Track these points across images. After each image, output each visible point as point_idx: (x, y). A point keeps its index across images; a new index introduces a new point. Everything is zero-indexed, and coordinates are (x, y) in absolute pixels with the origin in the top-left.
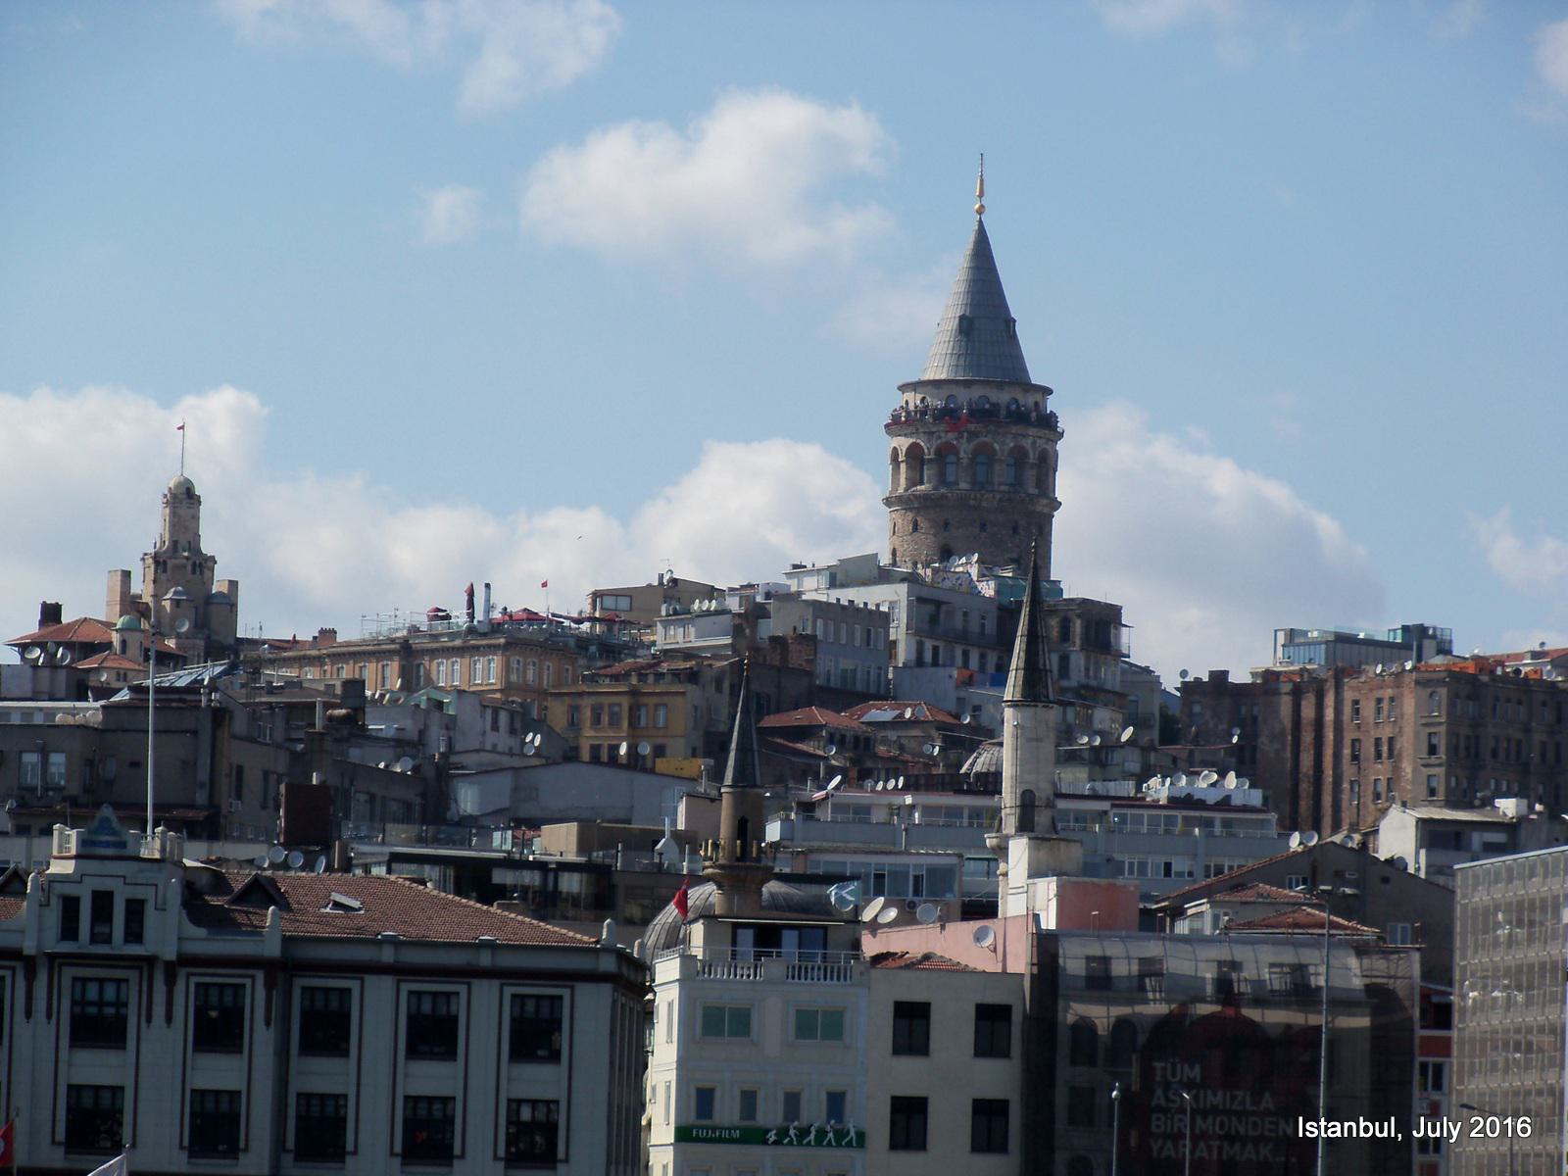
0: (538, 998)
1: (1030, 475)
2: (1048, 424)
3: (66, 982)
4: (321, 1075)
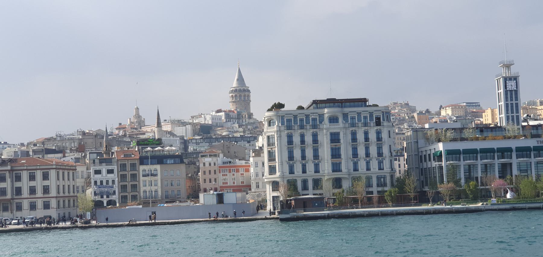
0: (46, 172)
1: (246, 98)
2: (249, 91)
4: (18, 184)
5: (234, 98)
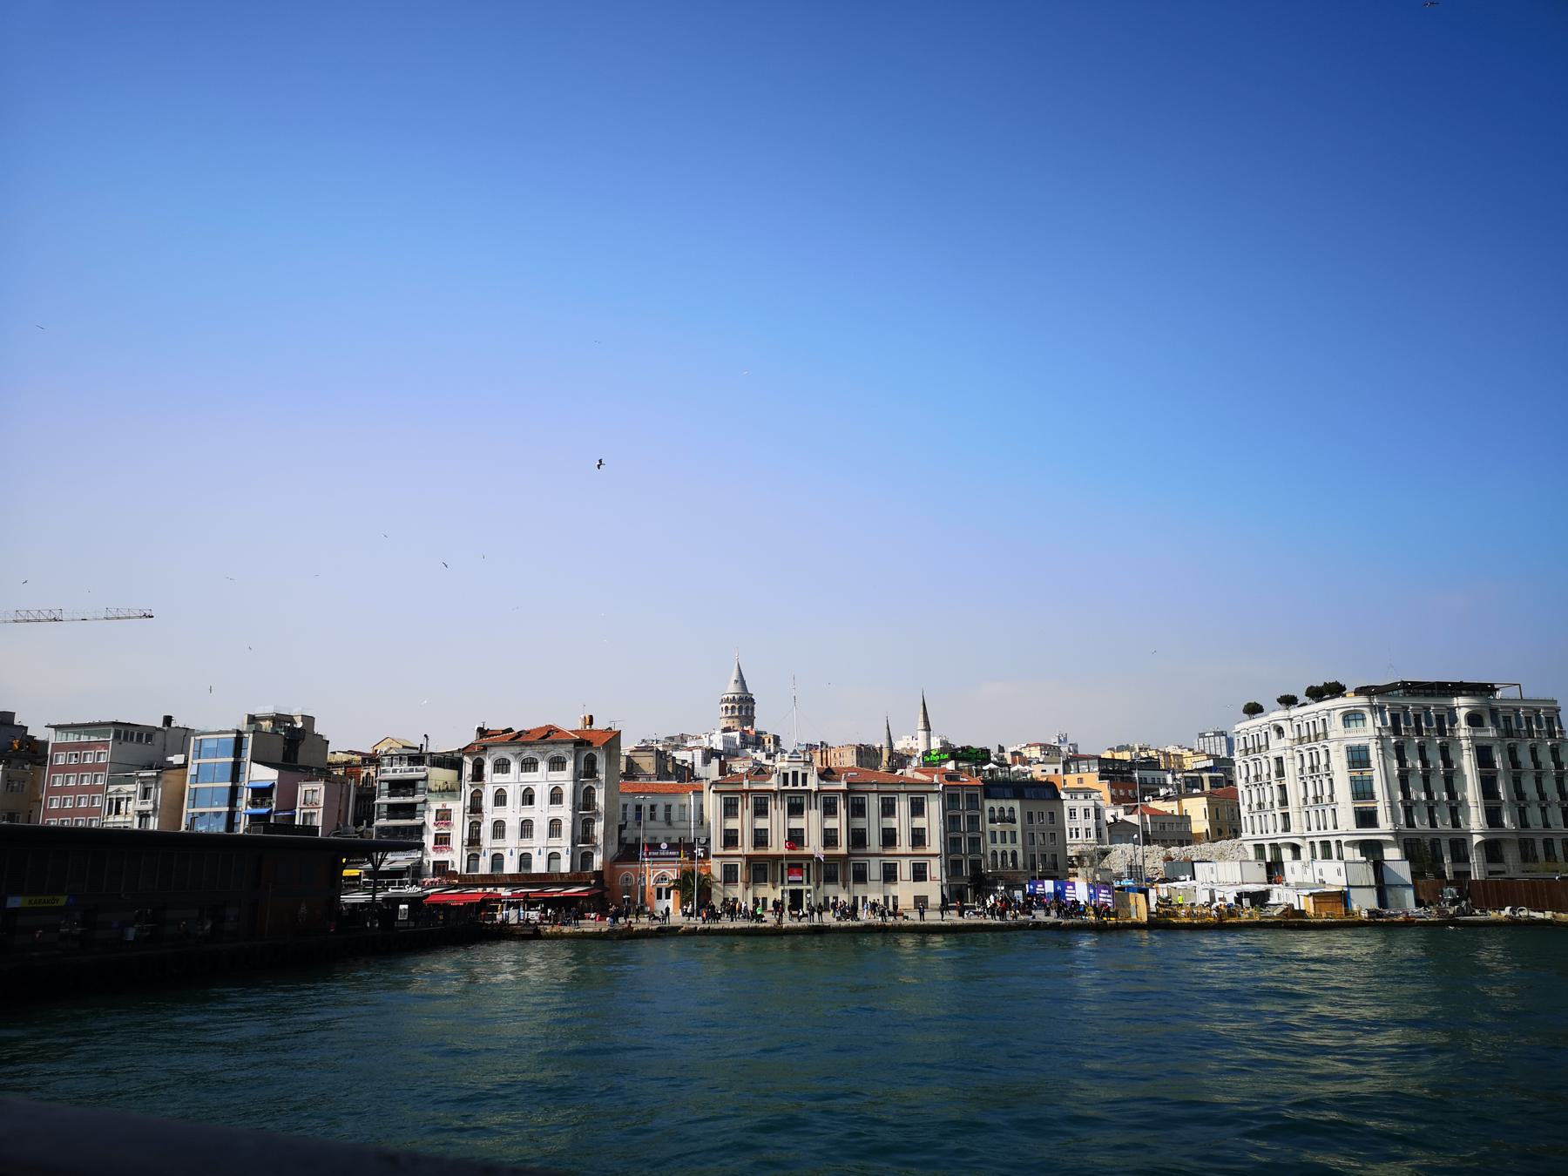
1: (750, 711)
3: (786, 798)
4: (859, 823)
5: (729, 711)
